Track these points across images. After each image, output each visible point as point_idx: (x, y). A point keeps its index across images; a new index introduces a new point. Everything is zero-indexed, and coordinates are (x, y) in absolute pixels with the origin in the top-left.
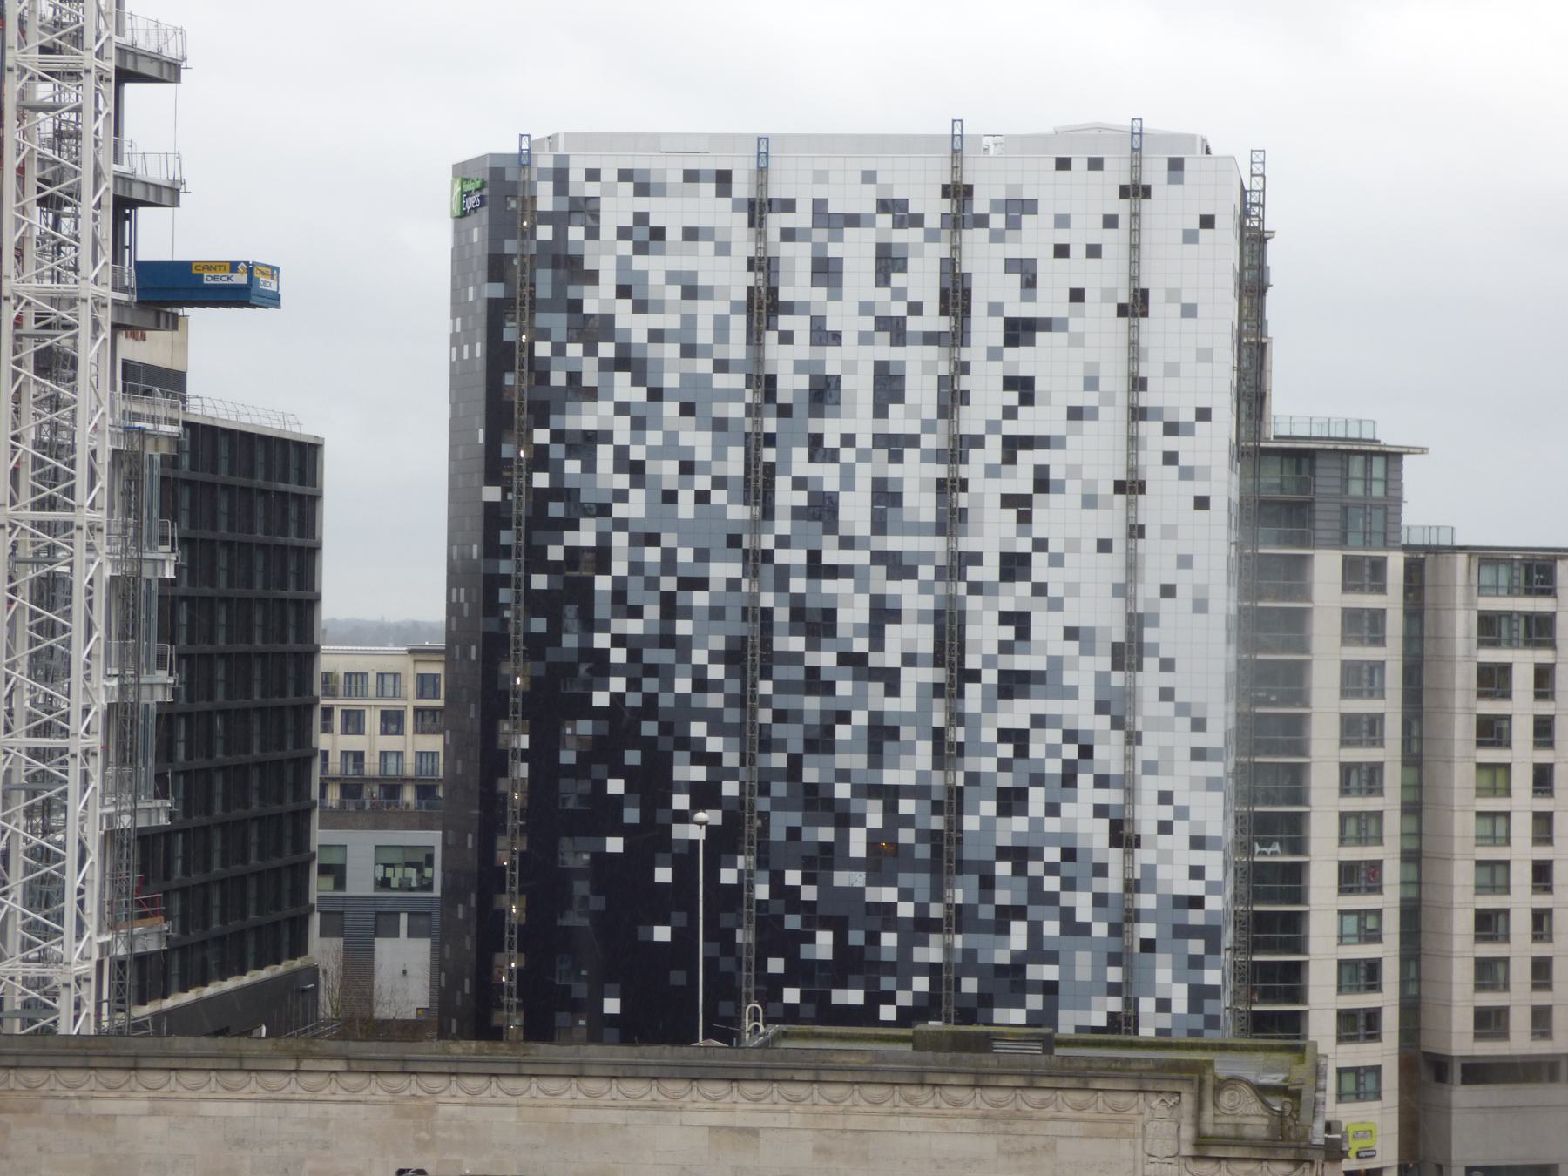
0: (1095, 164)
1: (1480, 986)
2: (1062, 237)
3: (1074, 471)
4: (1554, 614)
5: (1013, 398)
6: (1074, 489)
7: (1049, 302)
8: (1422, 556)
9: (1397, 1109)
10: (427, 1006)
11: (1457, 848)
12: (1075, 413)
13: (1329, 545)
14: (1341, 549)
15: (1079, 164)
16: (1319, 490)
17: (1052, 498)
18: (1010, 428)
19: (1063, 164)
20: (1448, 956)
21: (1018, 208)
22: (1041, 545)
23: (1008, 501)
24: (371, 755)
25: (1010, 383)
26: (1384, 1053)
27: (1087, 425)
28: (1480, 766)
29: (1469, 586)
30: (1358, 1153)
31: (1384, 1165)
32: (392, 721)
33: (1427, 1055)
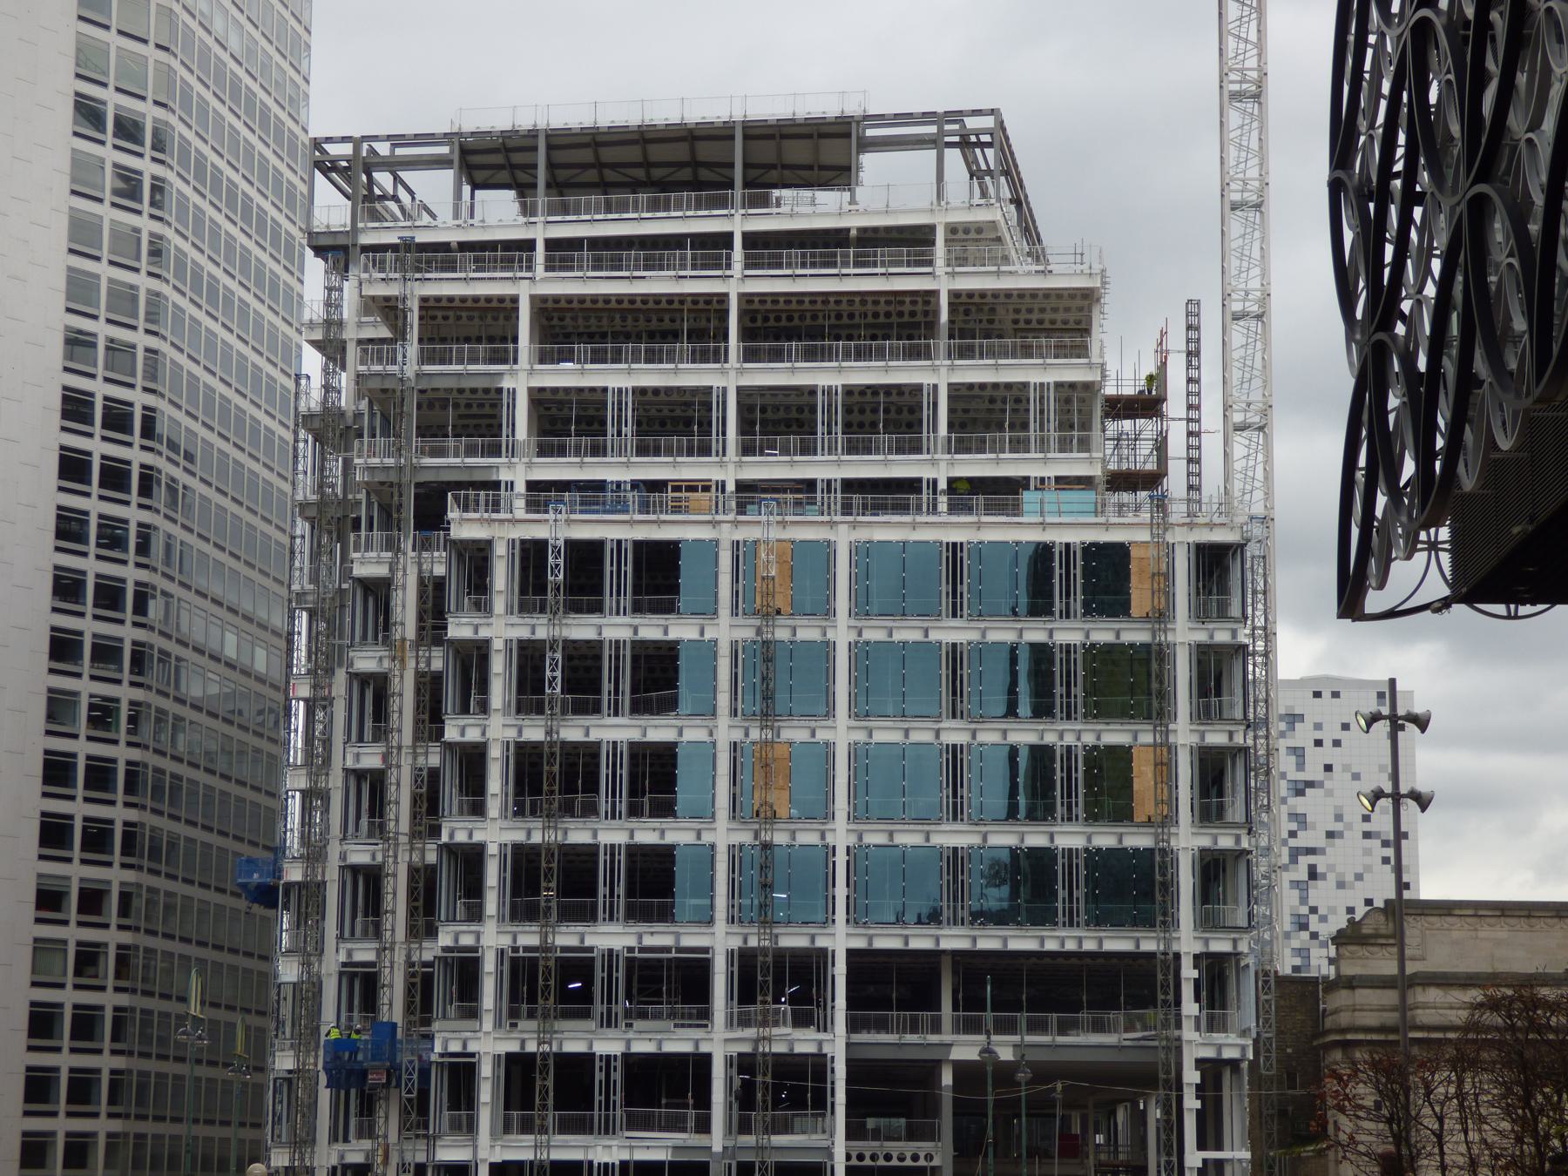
0: (1336, 695)
2: (1318, 735)
3: (1331, 868)
5: (1294, 826)
6: (1331, 877)
7: (1313, 772)
12: (1330, 835)
15: (1326, 694)
17: (1320, 883)
18: (1293, 843)
19: (1317, 695)
21: (1293, 719)
22: (1314, 910)
23: (1296, 884)
25: (1294, 816)
27: (1337, 841)
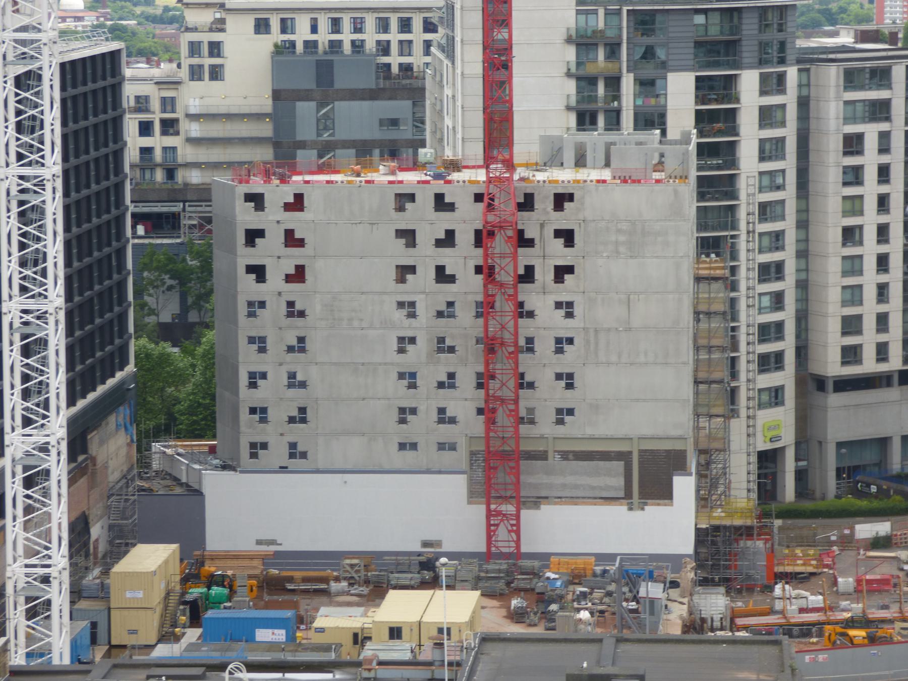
1: (844, 333)
4: (890, 99)
8: (808, 66)
9: (794, 410)
10: (179, 312)
11: (831, 250)
13: (751, 67)
14: (759, 69)
16: (744, 32)
20: (825, 316)
24: (135, 150)
26: (785, 378)
28: (845, 198)
29: (838, 86)
30: (771, 439)
31: (787, 444)
32: (145, 129)
33: (811, 374)
